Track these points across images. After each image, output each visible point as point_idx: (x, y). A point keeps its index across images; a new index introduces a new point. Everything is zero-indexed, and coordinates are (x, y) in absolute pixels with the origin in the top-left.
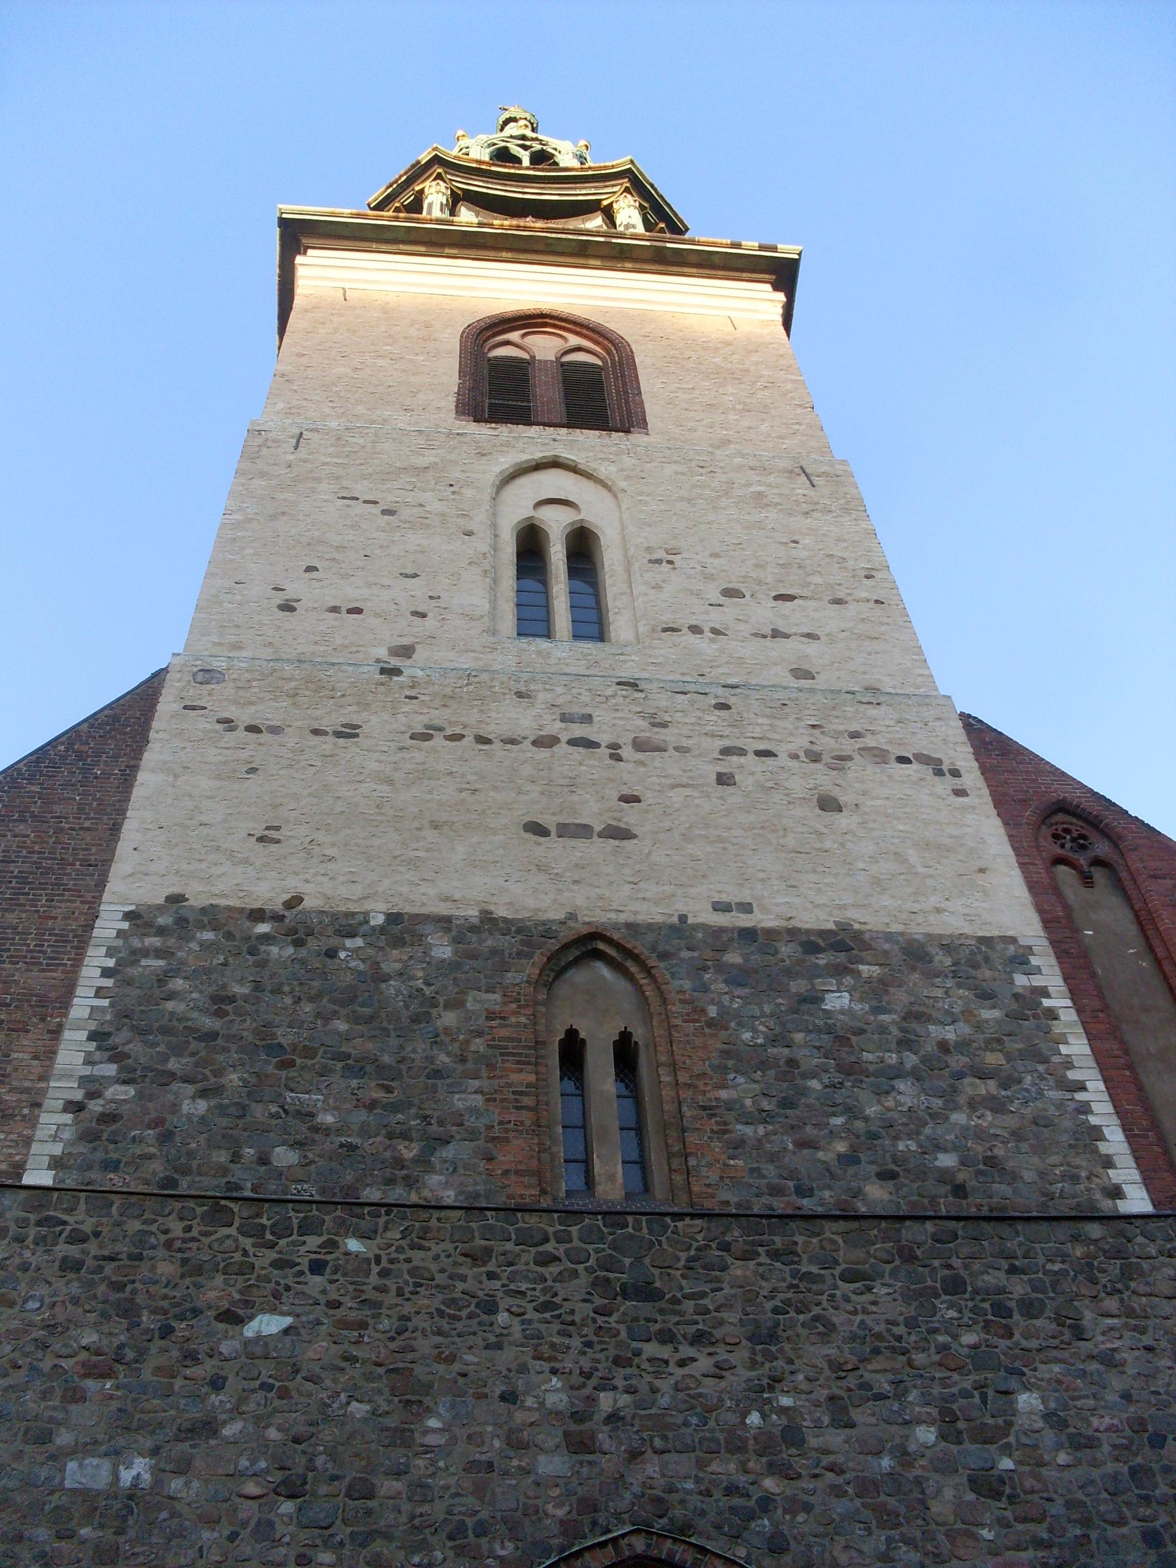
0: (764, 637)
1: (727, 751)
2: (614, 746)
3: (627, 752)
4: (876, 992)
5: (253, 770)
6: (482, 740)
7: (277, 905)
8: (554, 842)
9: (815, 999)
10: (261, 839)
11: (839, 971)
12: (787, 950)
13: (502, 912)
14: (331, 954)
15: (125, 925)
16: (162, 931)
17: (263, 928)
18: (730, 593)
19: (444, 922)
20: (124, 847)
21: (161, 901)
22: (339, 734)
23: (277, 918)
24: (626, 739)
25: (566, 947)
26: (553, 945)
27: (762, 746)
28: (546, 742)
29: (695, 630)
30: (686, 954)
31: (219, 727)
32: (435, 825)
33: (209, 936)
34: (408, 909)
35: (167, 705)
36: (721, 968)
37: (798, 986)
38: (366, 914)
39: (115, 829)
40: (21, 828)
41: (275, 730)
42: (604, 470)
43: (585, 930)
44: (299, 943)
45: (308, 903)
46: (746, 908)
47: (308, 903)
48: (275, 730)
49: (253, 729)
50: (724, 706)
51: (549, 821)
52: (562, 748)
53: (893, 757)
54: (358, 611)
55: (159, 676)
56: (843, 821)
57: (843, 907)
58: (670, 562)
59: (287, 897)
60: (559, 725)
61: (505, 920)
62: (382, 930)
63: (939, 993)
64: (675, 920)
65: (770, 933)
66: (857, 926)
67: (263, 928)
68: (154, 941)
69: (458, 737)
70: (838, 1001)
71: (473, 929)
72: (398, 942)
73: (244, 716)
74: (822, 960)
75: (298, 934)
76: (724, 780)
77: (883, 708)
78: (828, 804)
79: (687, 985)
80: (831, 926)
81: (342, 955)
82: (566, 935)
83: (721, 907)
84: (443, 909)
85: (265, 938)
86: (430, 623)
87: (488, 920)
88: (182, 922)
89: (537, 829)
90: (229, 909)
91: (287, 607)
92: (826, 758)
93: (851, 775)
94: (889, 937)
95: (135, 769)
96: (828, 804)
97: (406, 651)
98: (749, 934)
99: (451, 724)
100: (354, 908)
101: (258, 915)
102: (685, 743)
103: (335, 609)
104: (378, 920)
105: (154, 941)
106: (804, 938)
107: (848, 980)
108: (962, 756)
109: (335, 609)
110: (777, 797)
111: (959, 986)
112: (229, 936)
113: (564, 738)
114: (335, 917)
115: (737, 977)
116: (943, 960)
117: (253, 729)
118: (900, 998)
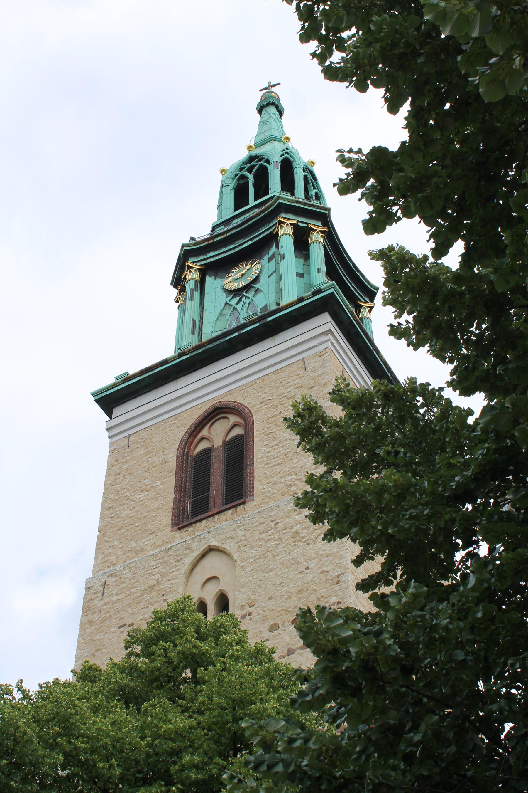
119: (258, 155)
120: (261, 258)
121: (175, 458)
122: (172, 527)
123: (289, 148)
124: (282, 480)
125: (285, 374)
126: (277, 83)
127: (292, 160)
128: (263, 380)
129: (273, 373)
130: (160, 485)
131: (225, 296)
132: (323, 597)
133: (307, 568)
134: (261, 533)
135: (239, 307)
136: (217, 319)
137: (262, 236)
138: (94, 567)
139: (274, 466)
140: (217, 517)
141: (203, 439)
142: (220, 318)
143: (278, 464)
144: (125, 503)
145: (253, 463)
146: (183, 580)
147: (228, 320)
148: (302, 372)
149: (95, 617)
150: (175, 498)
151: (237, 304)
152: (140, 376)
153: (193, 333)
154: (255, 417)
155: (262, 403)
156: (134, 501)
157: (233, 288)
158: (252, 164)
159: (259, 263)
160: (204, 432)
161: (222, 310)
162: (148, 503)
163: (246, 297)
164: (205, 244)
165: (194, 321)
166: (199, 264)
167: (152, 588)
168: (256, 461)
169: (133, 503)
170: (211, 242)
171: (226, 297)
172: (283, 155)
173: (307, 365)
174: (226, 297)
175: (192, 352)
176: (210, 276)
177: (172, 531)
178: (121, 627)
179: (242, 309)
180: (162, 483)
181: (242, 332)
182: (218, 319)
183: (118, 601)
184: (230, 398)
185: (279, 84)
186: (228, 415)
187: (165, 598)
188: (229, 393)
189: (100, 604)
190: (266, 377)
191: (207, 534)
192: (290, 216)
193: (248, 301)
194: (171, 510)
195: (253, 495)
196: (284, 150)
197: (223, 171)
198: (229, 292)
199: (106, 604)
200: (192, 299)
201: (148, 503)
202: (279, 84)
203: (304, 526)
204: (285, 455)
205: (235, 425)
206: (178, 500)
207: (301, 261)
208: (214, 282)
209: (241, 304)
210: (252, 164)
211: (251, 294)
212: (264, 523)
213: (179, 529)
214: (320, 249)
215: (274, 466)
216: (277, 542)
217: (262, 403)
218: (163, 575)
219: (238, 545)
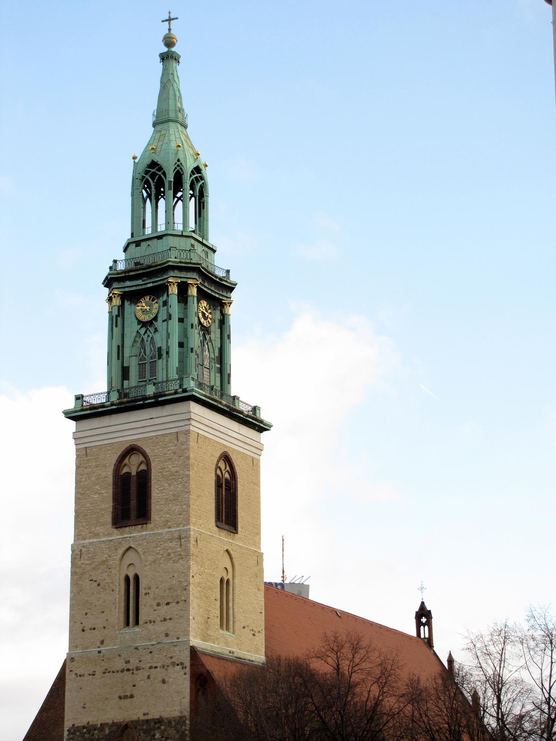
0: (162, 621)
1: (151, 668)
2: (133, 670)
3: (135, 672)
4: (162, 733)
5: (81, 689)
6: (113, 672)
7: (86, 724)
8: (123, 701)
9: (154, 735)
10: (84, 708)
11: (159, 728)
12: (152, 724)
13: (115, 721)
14: (93, 735)
15: (68, 733)
16: (72, 734)
17: (85, 730)
18: (158, 604)
19: (107, 724)
20: (66, 713)
21: (71, 726)
22: (93, 675)
23: (86, 728)
24: (134, 668)
25: (123, 727)
26: (121, 728)
27: (156, 665)
28: (122, 671)
29: (150, 622)
30: (139, 727)
31: (75, 676)
32: (107, 699)
33: (78, 733)
34: (103, 722)
35: (67, 671)
36: (143, 730)
37: (152, 733)
38: (97, 724)
39: (64, 708)
40: (52, 711)
41: (83, 675)
42: (140, 549)
43: (126, 723)
44: (89, 733)
45: (90, 723)
46: (148, 714)
47: (90, 723)
48: (83, 675)
49: (80, 676)
50: (151, 652)
51: (122, 695)
52: (125, 672)
53: (176, 664)
54: (94, 629)
55: (65, 660)
56: (165, 686)
57: (161, 712)
58: (149, 594)
59: (87, 722)
60: (125, 665)
61: (116, 723)
62: (99, 728)
63: (170, 732)
64: (138, 719)
65: (150, 720)
66: (162, 717)
67: (85, 730)
68: (71, 736)
69: (109, 672)
70: (158, 736)
71: (111, 726)
72: (102, 731)
73: (79, 674)
74: (157, 726)
75: (89, 731)
76: (149, 677)
77: (177, 647)
78: (164, 682)
79: (138, 734)
80: (159, 717)
81: (95, 735)
82: (123, 725)
83: (144, 715)
84: (108, 721)
85: (85, 733)
86: (106, 630)
87: (114, 724)
88: (74, 731)
89: (120, 698)
90: (80, 726)
91: (83, 630)
92: (166, 667)
93: (169, 671)
94: (167, 719)
95: (64, 691)
96: (164, 682)
97: (102, 642)
98: (147, 721)
99: (109, 667)
100: (96, 723)
101: (84, 727)
102: (144, 666)
103: (91, 629)
104: (99, 726)
105: (71, 736)
106: (154, 721)
107: (160, 730)
108: (187, 663)
109: (91, 629)
110: (156, 681)
111: (174, 730)
112: (81, 733)
113: (125, 669)
114: (93, 725)
115: (145, 732)
116: (173, 723)
117: (80, 676)
118: (166, 734)
119: (158, 163)
120: (158, 298)
121: (112, 476)
122: (112, 525)
123: (181, 159)
124: (164, 516)
125: (167, 439)
126: (175, 17)
127: (182, 173)
128: (157, 438)
129: (162, 435)
130: (105, 493)
131: (137, 323)
132: (179, 595)
133: (173, 577)
134: (154, 548)
135: (145, 337)
136: (133, 345)
137: (159, 283)
138: (75, 536)
139: (161, 504)
140: (134, 527)
141: (125, 465)
142: (134, 344)
143: (163, 504)
144: (87, 499)
145: (151, 498)
146: (117, 562)
147: (139, 347)
148: (175, 442)
149: (78, 570)
150: (113, 505)
151: (144, 335)
152: (90, 410)
153: (118, 359)
154: (152, 464)
155: (156, 456)
156: (92, 499)
157: (141, 319)
158: (154, 170)
159: (157, 302)
160: (126, 461)
161: (135, 337)
162: (99, 503)
163: (149, 331)
164: (123, 275)
165: (118, 346)
166: (120, 290)
167: (103, 562)
168: (152, 498)
169: (91, 499)
170: (127, 274)
171: (138, 325)
172: (176, 168)
173: (178, 438)
174: (138, 325)
175: (118, 405)
176: (128, 301)
177: (112, 528)
178: (91, 580)
179: (147, 341)
180: (106, 492)
181: (145, 402)
182: (133, 346)
183: (87, 564)
184: (139, 444)
185: (177, 18)
186: (139, 454)
187: (110, 570)
188: (139, 440)
189: (80, 563)
190: (158, 436)
191: (129, 538)
192: (177, 273)
193: (151, 336)
194: (111, 513)
195: (150, 520)
196: (176, 163)
197: (134, 158)
198: (139, 322)
199: (83, 564)
200: (116, 326)
201: (99, 503)
202: (177, 18)
203: (172, 551)
204: (166, 499)
205: (142, 463)
206: (115, 508)
207: (183, 305)
208: (129, 307)
209: (146, 335)
210: (154, 170)
211: (152, 329)
212: (155, 542)
213: (116, 528)
214: (194, 303)
215: (161, 504)
216: (161, 556)
217: (156, 456)
218: (110, 556)
219: (144, 550)
